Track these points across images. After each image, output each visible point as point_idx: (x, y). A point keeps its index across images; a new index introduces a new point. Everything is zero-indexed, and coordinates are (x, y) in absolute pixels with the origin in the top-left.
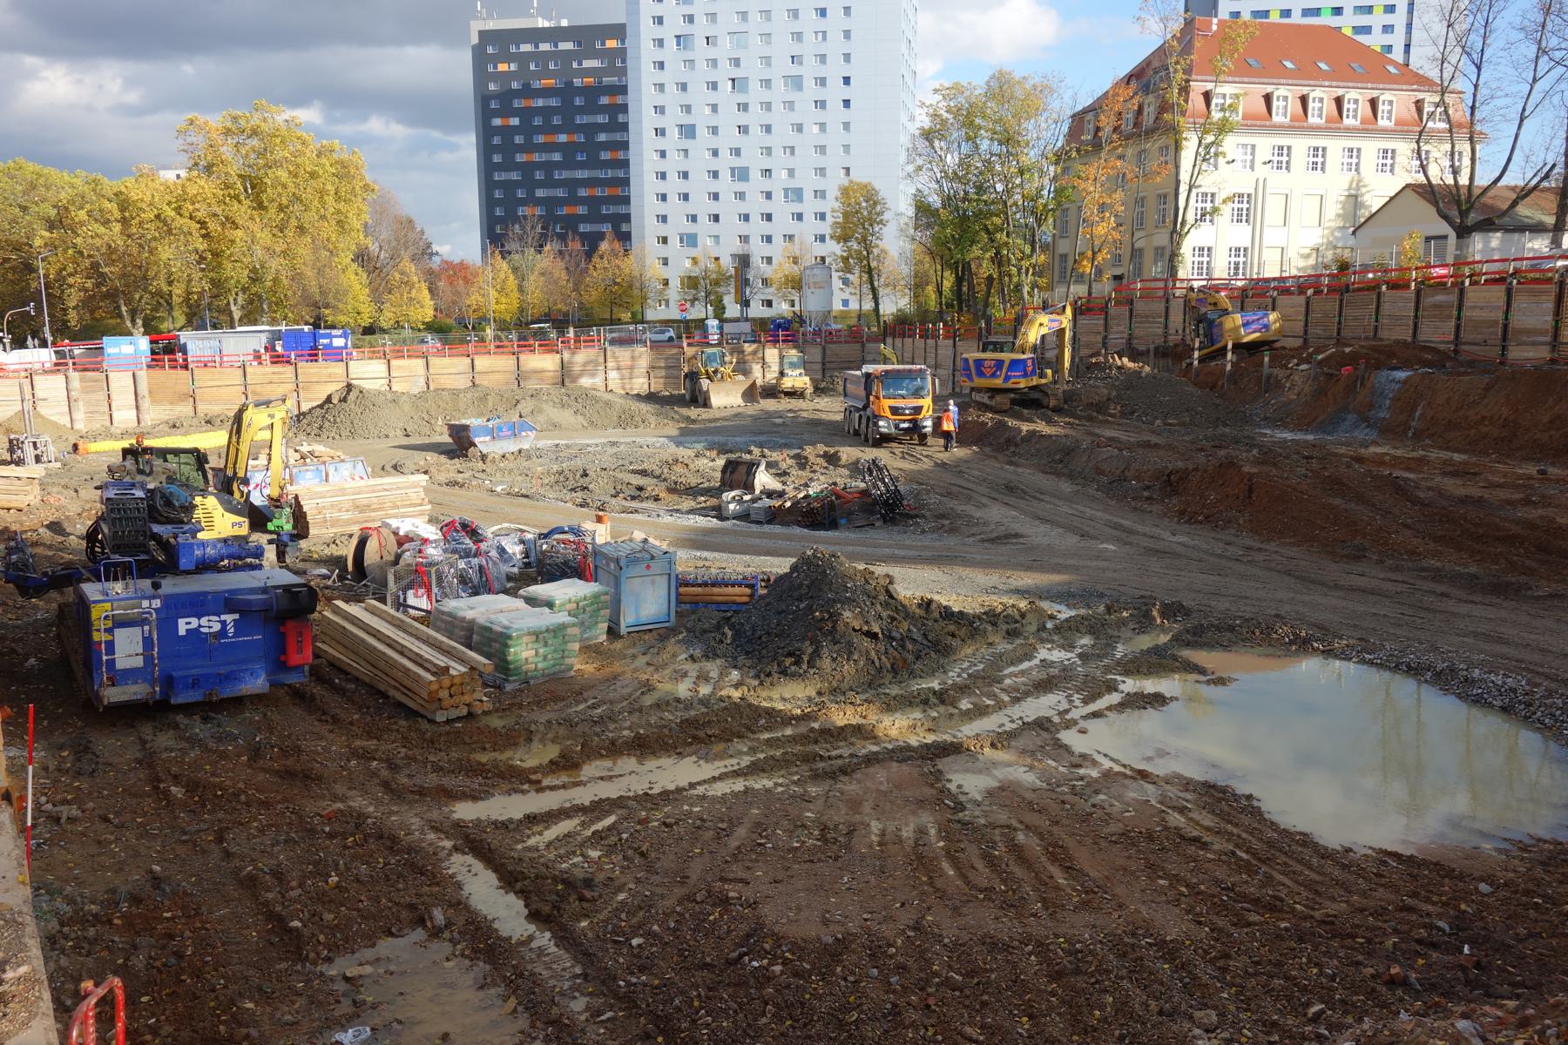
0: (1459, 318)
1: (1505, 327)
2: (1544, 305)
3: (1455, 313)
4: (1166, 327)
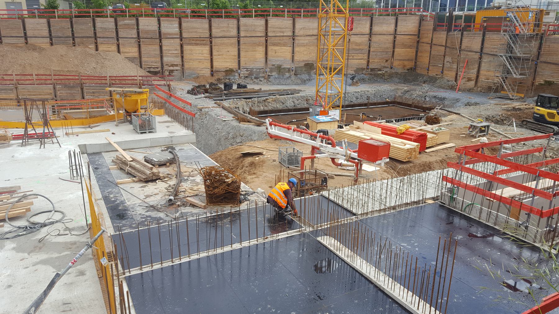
0: (138, 29)
1: (160, 33)
2: (175, 25)
3: (136, 27)
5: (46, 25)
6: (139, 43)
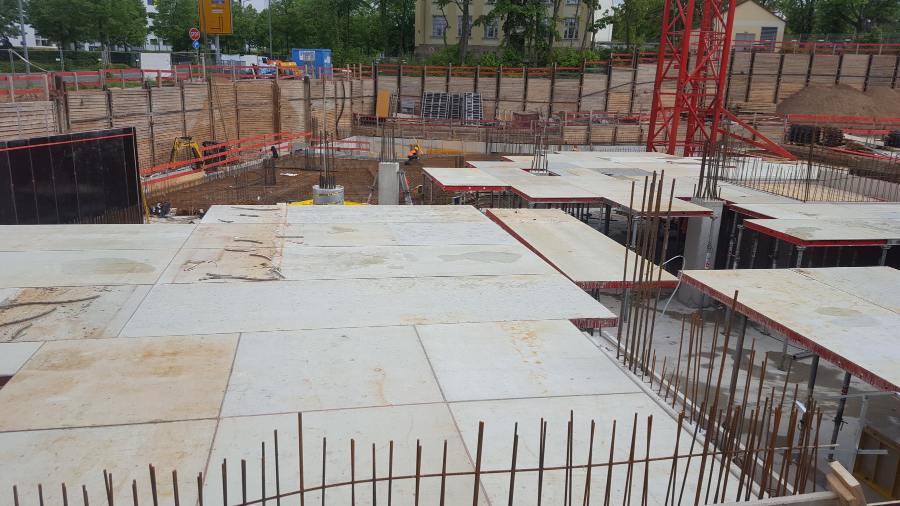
5: (866, 63)
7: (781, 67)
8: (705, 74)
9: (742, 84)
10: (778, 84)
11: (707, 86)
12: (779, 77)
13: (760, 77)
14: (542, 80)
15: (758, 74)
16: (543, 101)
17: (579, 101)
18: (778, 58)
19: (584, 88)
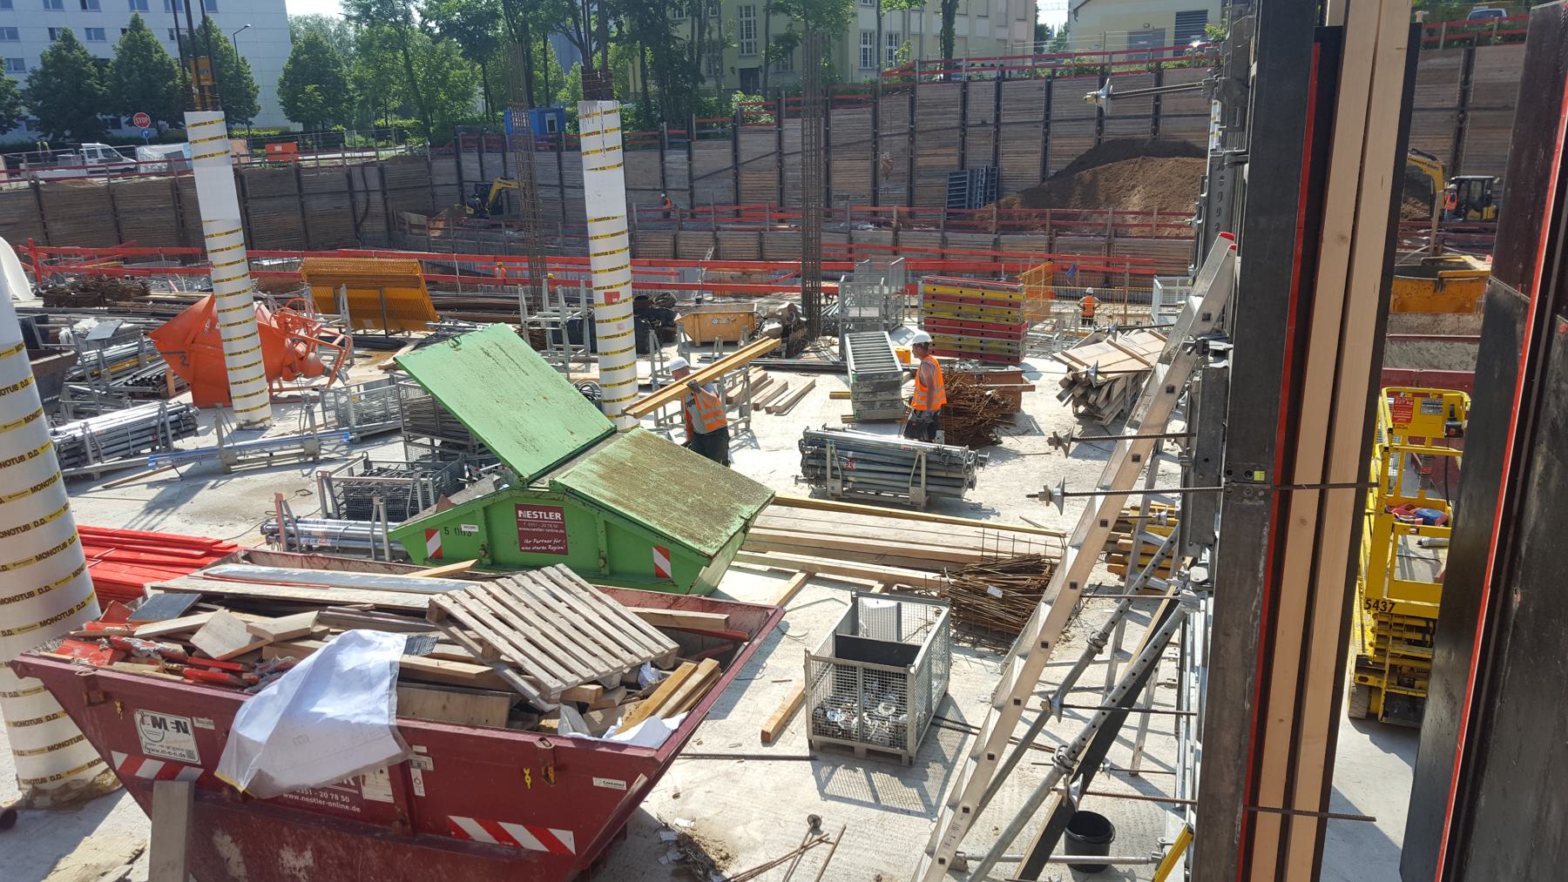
0: (1466, 81)
3: (1460, 76)
4: (964, 116)
6: (1461, 123)
7: (1048, 107)
8: (912, 129)
9: (985, 144)
10: (1046, 141)
11: (919, 152)
12: (1047, 126)
13: (1013, 128)
14: (646, 153)
15: (1009, 124)
16: (651, 187)
17: (691, 187)
18: (1041, 89)
19: (696, 165)
